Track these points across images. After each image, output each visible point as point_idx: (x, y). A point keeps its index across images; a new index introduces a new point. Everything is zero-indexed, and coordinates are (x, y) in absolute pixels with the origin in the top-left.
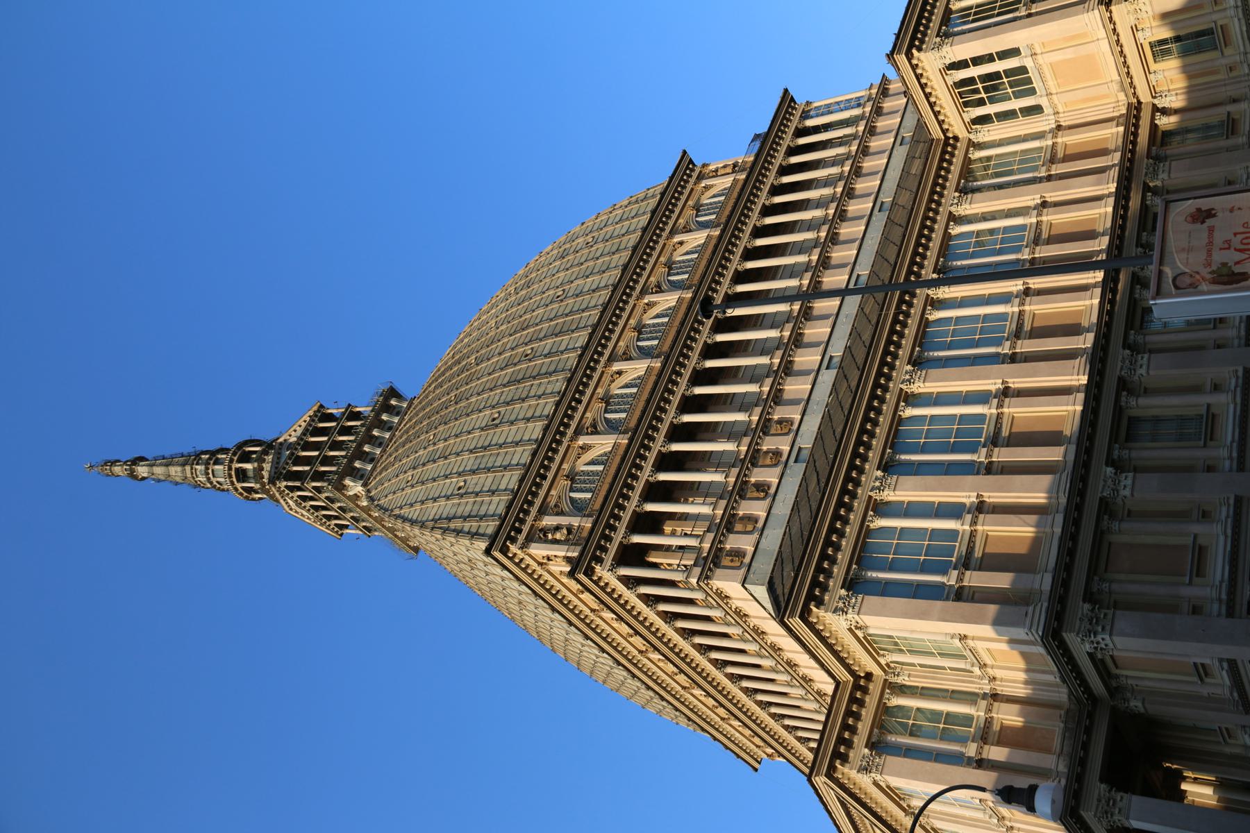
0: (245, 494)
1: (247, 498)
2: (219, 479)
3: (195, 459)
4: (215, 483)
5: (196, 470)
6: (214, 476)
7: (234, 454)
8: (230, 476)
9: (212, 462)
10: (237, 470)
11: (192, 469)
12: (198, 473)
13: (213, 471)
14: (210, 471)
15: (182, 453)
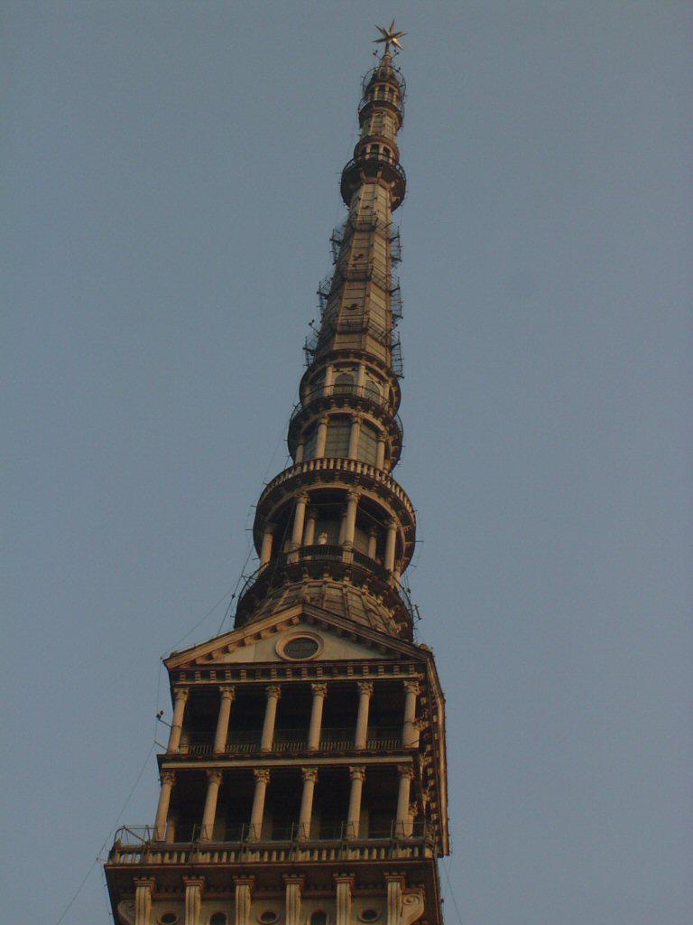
0: (275, 507)
1: (262, 509)
2: (323, 432)
3: (381, 365)
4: (313, 418)
5: (358, 365)
6: (334, 417)
7: (384, 492)
8: (328, 475)
9: (369, 417)
10: (341, 498)
11: (358, 354)
12: (345, 370)
13: (348, 417)
14: (347, 410)
15: (400, 317)
